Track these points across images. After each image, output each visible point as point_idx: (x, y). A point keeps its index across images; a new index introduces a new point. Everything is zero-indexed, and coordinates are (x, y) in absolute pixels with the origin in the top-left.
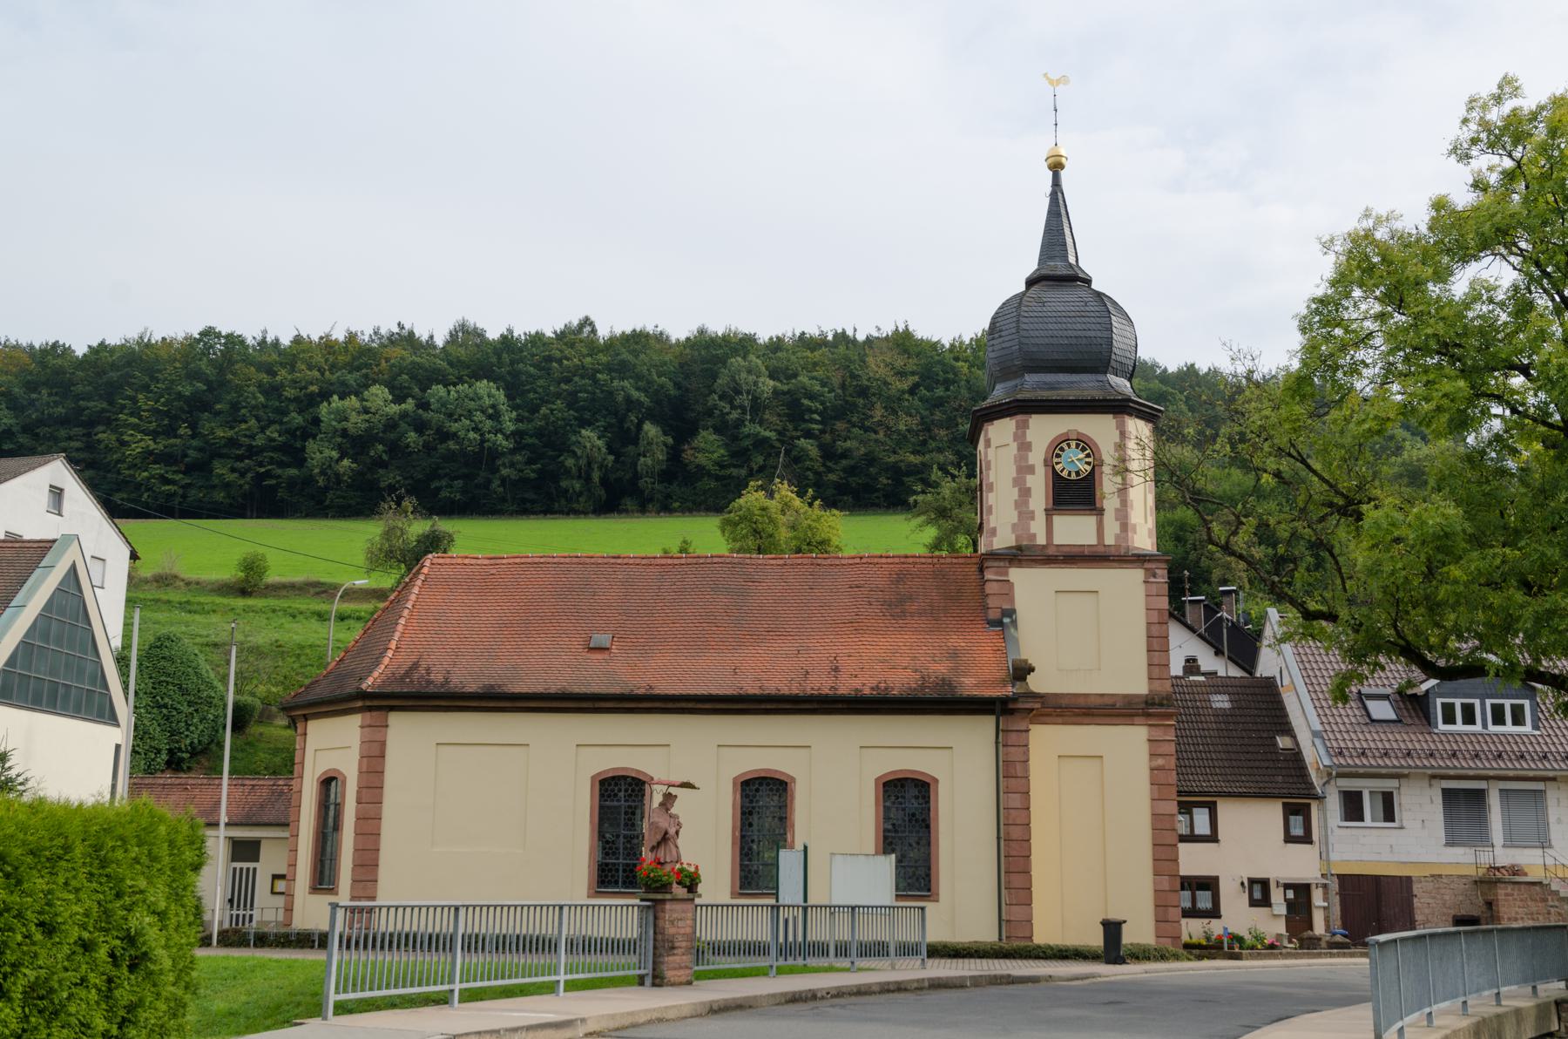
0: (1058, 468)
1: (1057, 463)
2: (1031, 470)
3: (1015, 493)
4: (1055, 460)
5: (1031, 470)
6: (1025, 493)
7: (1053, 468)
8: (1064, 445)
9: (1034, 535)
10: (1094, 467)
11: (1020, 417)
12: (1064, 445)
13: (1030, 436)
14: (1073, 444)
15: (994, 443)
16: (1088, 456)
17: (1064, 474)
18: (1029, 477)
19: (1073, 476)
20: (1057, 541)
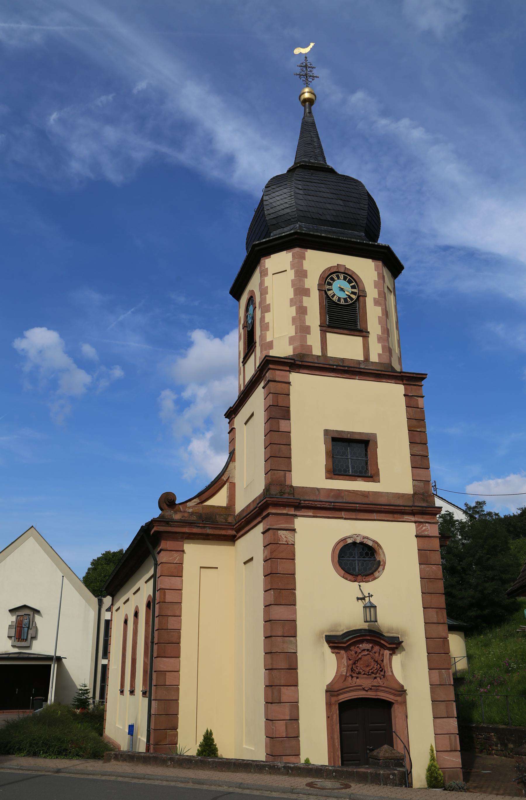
0: (329, 293)
1: (329, 290)
2: (306, 292)
3: (293, 311)
4: (328, 287)
5: (306, 292)
6: (302, 311)
7: (326, 293)
8: (334, 276)
9: (310, 347)
10: (358, 297)
11: (297, 250)
12: (334, 276)
13: (306, 265)
14: (342, 276)
15: (270, 272)
16: (353, 287)
17: (335, 299)
18: (305, 298)
19: (342, 302)
20: (331, 353)
